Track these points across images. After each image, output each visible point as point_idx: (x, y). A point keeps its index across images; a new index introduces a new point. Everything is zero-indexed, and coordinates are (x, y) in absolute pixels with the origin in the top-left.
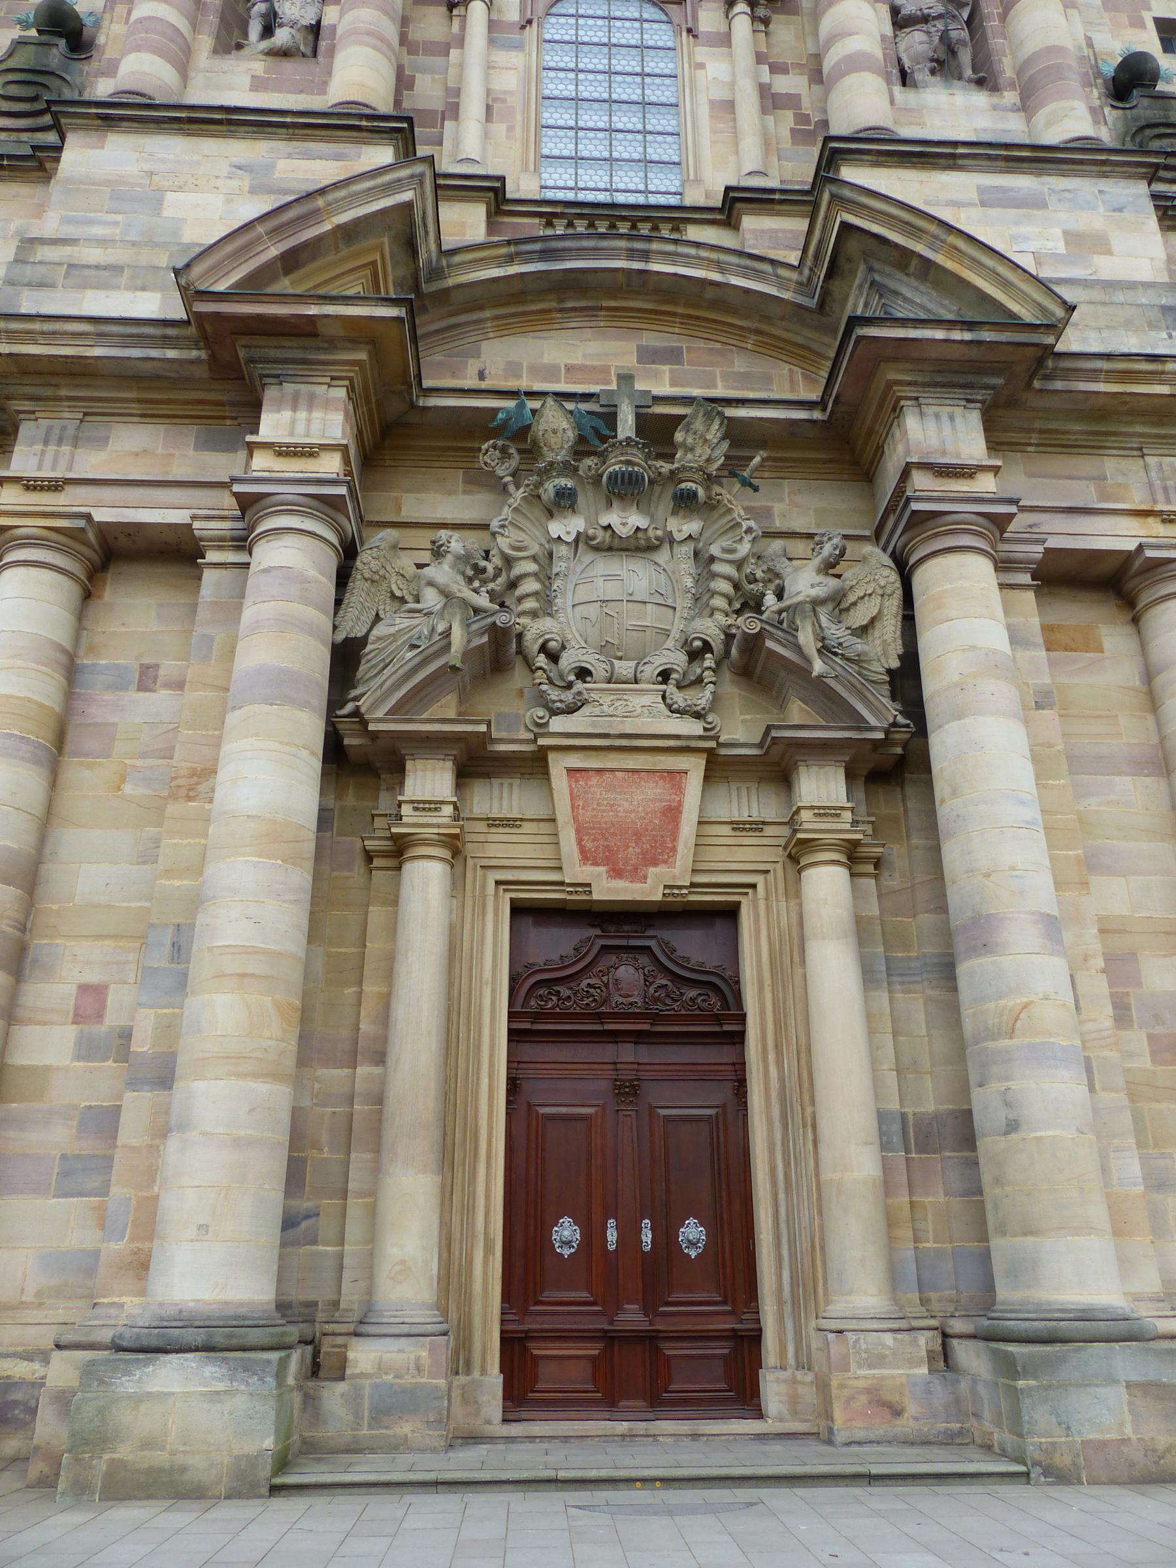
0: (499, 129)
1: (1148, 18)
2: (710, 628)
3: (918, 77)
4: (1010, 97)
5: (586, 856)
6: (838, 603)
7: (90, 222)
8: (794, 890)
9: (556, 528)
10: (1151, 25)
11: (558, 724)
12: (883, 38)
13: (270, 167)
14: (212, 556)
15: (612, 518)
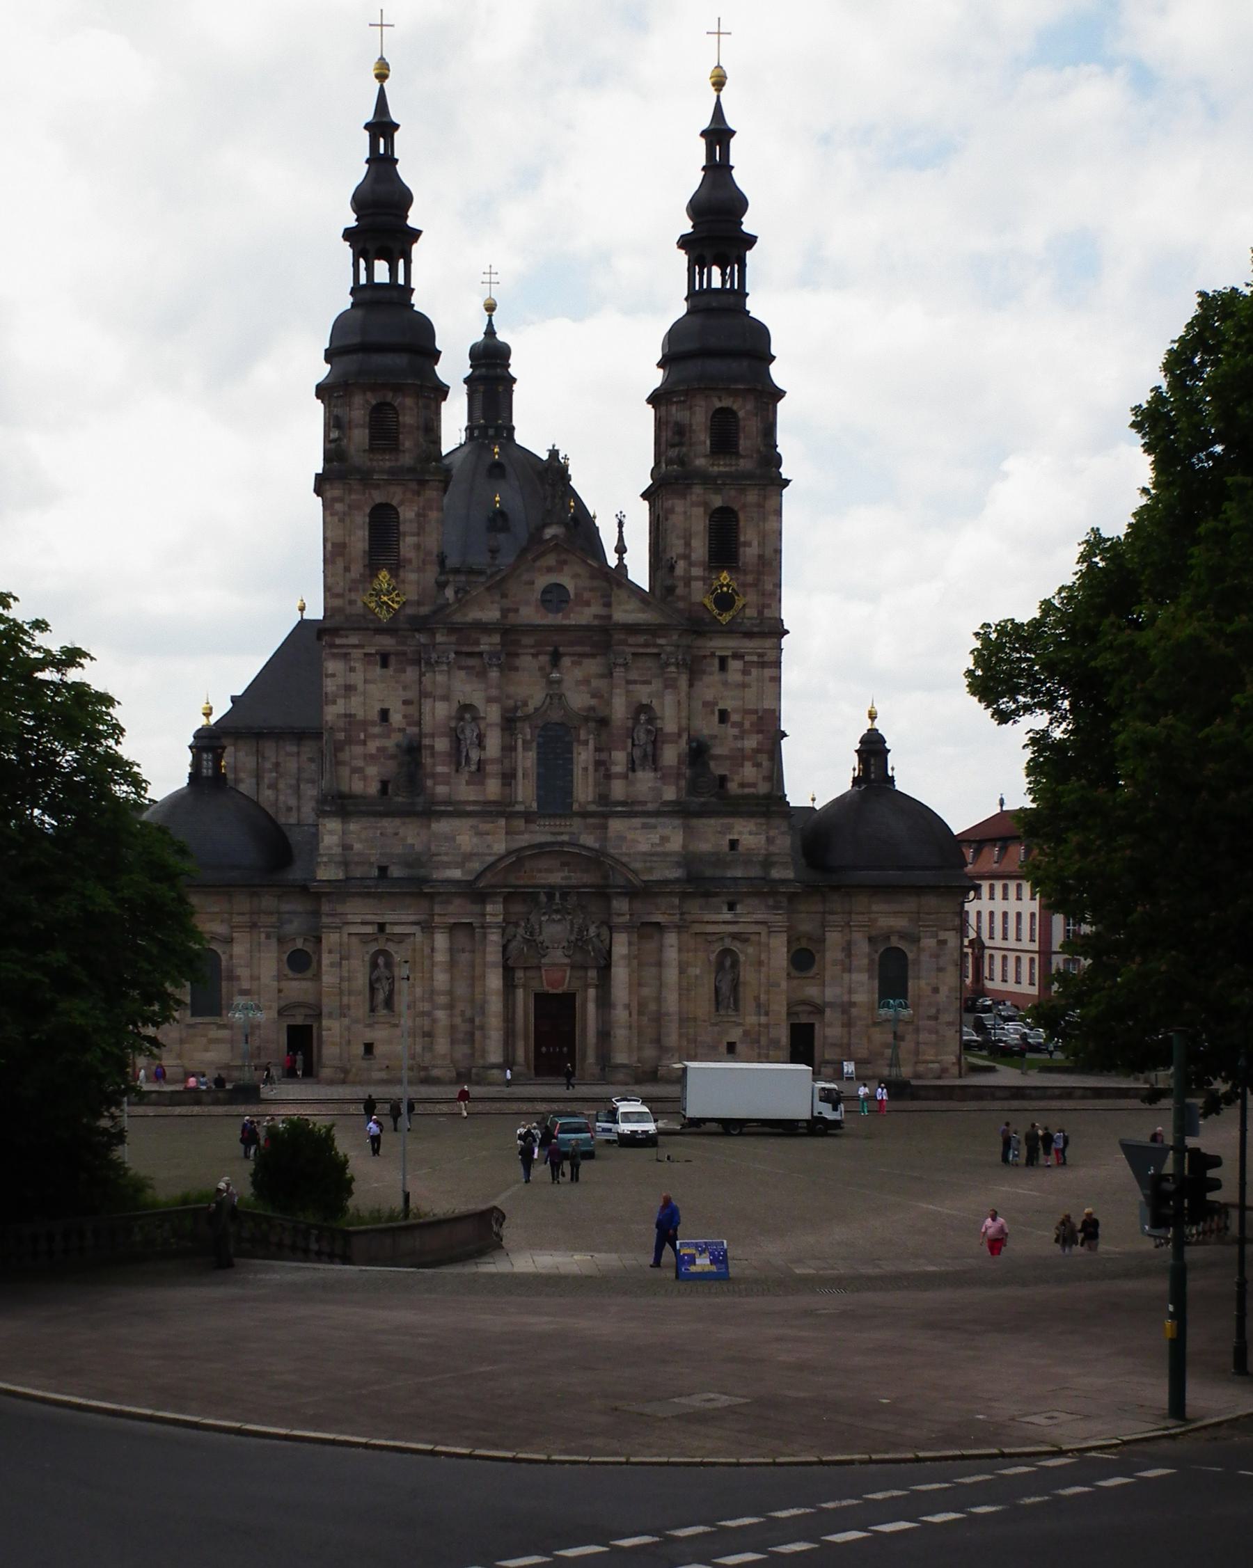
0: (526, 781)
1: (717, 708)
2: (573, 938)
3: (636, 767)
4: (659, 774)
5: (548, 985)
6: (598, 935)
7: (442, 846)
8: (586, 991)
9: (543, 918)
10: (717, 713)
11: (543, 961)
12: (628, 754)
13: (478, 827)
14: (477, 930)
15: (554, 917)
